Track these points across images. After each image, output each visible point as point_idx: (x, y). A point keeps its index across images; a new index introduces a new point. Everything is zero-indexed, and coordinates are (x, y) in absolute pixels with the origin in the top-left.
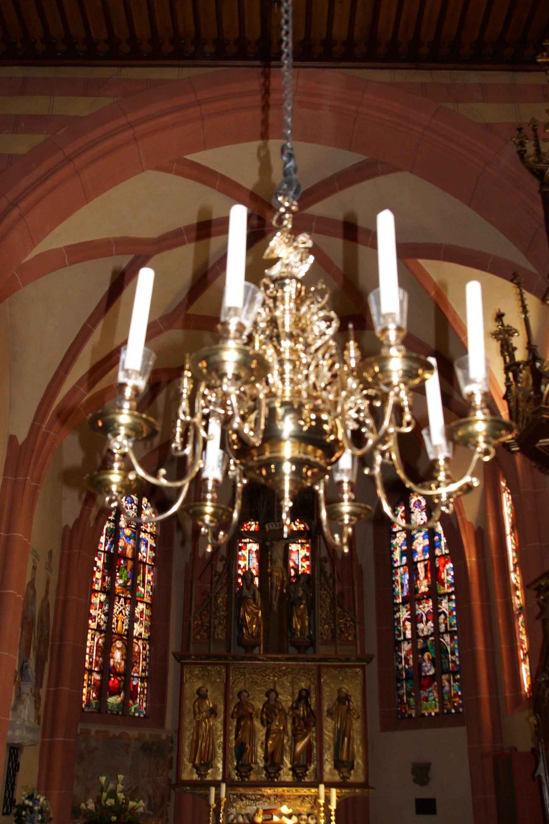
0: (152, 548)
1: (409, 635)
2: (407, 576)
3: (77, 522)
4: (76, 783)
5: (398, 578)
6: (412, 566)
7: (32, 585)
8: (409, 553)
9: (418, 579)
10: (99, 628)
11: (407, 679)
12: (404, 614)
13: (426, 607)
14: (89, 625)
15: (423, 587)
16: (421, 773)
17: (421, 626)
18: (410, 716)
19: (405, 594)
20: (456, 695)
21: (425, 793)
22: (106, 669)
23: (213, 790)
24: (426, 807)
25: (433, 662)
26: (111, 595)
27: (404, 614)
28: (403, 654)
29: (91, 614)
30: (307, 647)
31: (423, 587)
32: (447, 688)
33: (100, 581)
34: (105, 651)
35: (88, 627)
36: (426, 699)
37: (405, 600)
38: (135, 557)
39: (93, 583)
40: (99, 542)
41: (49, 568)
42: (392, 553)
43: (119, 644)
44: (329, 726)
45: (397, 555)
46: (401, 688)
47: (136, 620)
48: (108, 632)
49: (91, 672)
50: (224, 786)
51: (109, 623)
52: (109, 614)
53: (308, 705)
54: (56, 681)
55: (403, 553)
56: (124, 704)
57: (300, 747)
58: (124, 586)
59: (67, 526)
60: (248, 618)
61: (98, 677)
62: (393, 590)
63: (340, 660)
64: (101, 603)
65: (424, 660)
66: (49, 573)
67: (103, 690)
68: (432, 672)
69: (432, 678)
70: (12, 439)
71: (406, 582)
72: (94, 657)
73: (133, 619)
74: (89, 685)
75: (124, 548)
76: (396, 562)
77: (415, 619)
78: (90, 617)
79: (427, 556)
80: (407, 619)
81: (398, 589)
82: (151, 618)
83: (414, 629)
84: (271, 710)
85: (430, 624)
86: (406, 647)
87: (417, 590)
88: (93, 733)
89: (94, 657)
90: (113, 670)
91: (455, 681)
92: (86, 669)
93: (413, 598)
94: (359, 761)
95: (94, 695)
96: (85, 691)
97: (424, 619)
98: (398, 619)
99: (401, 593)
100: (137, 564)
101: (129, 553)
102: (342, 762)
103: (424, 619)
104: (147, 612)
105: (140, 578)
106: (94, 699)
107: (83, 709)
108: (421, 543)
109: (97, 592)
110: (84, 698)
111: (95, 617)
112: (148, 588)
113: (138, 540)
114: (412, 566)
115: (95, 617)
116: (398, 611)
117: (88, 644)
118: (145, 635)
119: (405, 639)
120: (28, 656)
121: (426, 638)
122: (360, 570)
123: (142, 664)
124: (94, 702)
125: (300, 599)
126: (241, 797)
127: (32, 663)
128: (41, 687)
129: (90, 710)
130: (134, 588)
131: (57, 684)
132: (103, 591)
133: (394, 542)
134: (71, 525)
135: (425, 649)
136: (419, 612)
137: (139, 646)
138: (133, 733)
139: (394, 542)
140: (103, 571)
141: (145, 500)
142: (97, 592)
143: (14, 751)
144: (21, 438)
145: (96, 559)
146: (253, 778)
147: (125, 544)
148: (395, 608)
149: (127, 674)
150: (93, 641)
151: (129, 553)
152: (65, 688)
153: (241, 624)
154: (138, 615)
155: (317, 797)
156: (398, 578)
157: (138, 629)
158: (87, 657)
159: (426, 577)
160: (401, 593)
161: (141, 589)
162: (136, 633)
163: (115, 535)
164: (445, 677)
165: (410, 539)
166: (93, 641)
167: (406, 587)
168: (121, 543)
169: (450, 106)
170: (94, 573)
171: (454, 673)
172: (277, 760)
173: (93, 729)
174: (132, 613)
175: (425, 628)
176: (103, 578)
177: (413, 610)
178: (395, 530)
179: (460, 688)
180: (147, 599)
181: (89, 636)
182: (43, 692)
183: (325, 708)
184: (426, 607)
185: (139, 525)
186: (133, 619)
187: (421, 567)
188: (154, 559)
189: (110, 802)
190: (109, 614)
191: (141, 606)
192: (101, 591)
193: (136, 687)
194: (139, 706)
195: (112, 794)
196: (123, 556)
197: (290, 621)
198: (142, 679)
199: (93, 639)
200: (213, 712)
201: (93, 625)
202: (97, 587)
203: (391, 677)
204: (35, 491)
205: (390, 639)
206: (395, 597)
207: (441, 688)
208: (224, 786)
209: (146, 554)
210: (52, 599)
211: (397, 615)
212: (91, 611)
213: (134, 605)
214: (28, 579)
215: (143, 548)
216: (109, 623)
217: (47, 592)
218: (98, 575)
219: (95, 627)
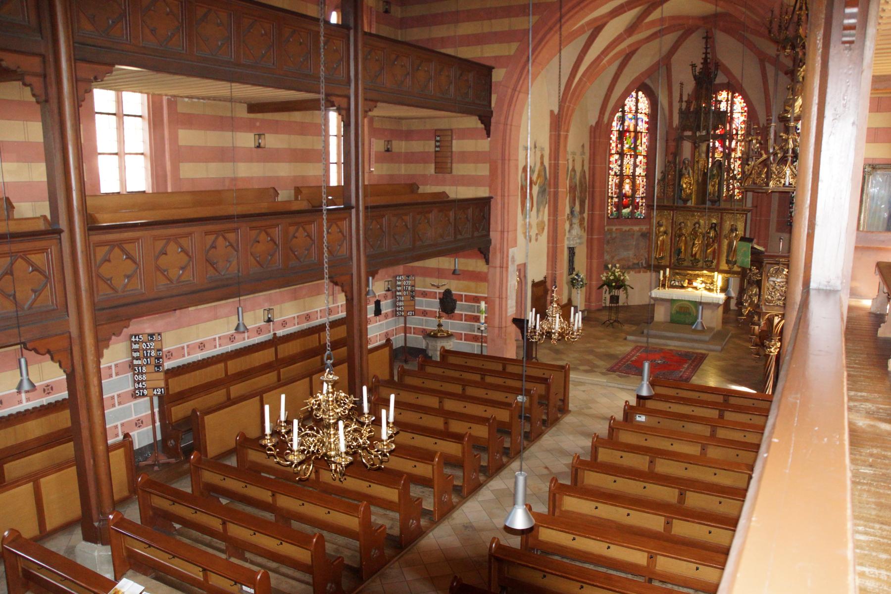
0: (646, 123)
3: (597, 123)
4: (605, 254)
7: (574, 170)
10: (616, 174)
22: (621, 195)
23: (662, 272)
26: (622, 154)
30: (715, 202)
34: (620, 186)
35: (609, 174)
38: (635, 131)
39: (610, 150)
40: (611, 126)
41: (583, 153)
43: (628, 181)
47: (637, 166)
48: (621, 176)
49: (612, 198)
50: (668, 270)
51: (621, 170)
52: (621, 166)
54: (592, 208)
56: (632, 212)
58: (630, 148)
60: (684, 186)
61: (616, 200)
64: (616, 161)
67: (619, 206)
70: (552, 112)
73: (635, 166)
75: (629, 126)
78: (610, 169)
82: (647, 164)
84: (694, 234)
90: (625, 195)
100: (636, 132)
101: (632, 129)
104: (645, 161)
105: (639, 142)
112: (644, 146)
113: (637, 119)
118: (643, 174)
120: (574, 204)
123: (642, 190)
124: (615, 213)
126: (677, 274)
127: (577, 208)
130: (636, 147)
131: (592, 210)
132: (617, 153)
134: (594, 124)
137: (639, 181)
138: (636, 228)
141: (640, 93)
143: (572, 251)
144: (556, 111)
146: (685, 264)
147: (629, 123)
149: (633, 196)
150: (613, 181)
151: (632, 129)
152: (597, 213)
153: (681, 189)
154: (638, 163)
157: (639, 171)
161: (639, 147)
162: (637, 174)
163: (622, 120)
166: (613, 181)
168: (626, 124)
173: (614, 228)
174: (635, 163)
176: (617, 146)
180: (644, 153)
182: (585, 215)
185: (636, 112)
186: (635, 166)
188: (647, 129)
189: (612, 278)
190: (621, 166)
191: (640, 158)
193: (638, 203)
194: (641, 212)
195: (613, 273)
196: (628, 131)
198: (642, 198)
200: (665, 233)
201: (612, 173)
202: (613, 152)
204: (566, 137)
208: (668, 270)
209: (642, 127)
210: (586, 168)
213: (636, 156)
214: (570, 168)
215: (640, 123)
216: (621, 170)
217: (583, 166)
218: (614, 145)
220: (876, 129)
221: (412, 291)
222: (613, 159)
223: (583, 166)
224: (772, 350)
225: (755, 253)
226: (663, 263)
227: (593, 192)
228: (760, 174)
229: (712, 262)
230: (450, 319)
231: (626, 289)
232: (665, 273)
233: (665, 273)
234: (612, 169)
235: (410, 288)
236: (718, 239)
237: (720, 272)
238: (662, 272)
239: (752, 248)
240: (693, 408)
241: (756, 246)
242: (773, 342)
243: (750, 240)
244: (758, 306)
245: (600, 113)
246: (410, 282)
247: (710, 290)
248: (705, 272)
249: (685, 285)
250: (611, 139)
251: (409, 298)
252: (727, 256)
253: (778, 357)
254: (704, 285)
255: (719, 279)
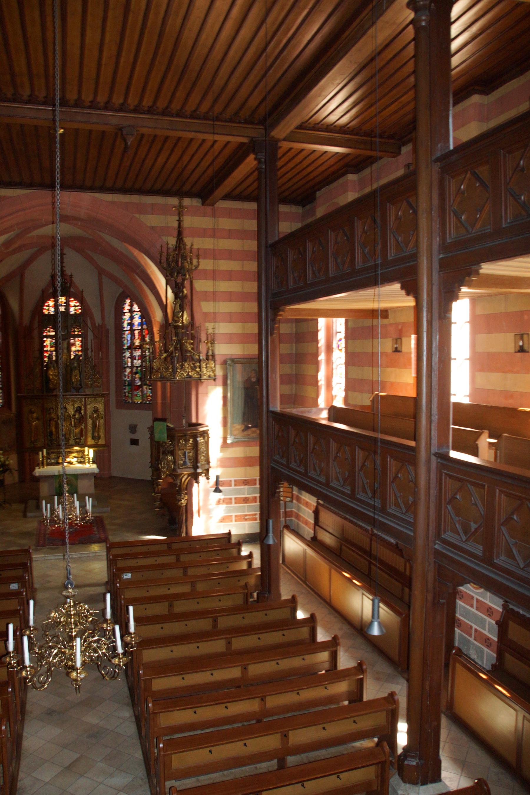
1: (129, 365)
2: (129, 336)
5: (125, 336)
6: (132, 331)
8: (131, 324)
9: (135, 339)
11: (128, 385)
12: (127, 354)
13: (138, 353)
15: (137, 343)
16: (133, 429)
17: (135, 361)
18: (129, 402)
19: (129, 345)
20: (149, 396)
21: (135, 437)
24: (135, 442)
25: (141, 379)
27: (127, 354)
28: (127, 373)
31: (137, 343)
32: (145, 392)
36: (136, 395)
37: (129, 348)
42: (124, 322)
44: (90, 422)
45: (125, 325)
46: (125, 389)
50: (45, 451)
53: (80, 413)
55: (129, 324)
57: (77, 430)
60: (51, 377)
62: (123, 342)
63: (93, 395)
65: (136, 378)
68: (139, 384)
69: (140, 387)
71: (129, 339)
76: (124, 328)
77: (133, 358)
79: (140, 328)
80: (129, 357)
81: (125, 342)
83: (132, 362)
85: (140, 361)
86: (128, 370)
87: (134, 344)
91: (150, 389)
93: (132, 347)
94: (102, 435)
97: (137, 358)
98: (125, 356)
99: (127, 344)
102: (95, 437)
103: (137, 358)
108: (137, 320)
114: (132, 331)
116: (125, 353)
119: (128, 367)
121: (137, 367)
122: (107, 331)
125: (75, 367)
133: (124, 317)
135: (136, 373)
136: (134, 355)
139: (124, 317)
148: (123, 351)
155: (84, 452)
156: (125, 336)
159: (138, 338)
160: (127, 344)
164: (145, 387)
165: (132, 318)
167: (129, 341)
169: (137, 216)
171: (150, 386)
172: (68, 436)
175: (137, 363)
177: (131, 353)
178: (125, 311)
179: (151, 393)
183: (88, 415)
184: (138, 353)
187: (136, 332)
197: (71, 377)
203: (120, 383)
205: (121, 367)
206: (124, 345)
207: (142, 392)
208: (45, 451)
211: (124, 355)
220: (231, 334)
224: (183, 501)
225: (169, 429)
226: (39, 444)
228: (167, 369)
229: (81, 439)
231: (11, 472)
232: (43, 454)
233: (43, 454)
236: (82, 419)
237: (90, 447)
238: (40, 453)
239: (167, 426)
240: (156, 559)
241: (169, 425)
242: (183, 496)
243: (164, 420)
244: (174, 470)
247: (80, 463)
248: (76, 448)
249: (60, 461)
252: (93, 433)
253: (186, 506)
254: (76, 459)
255: (90, 453)
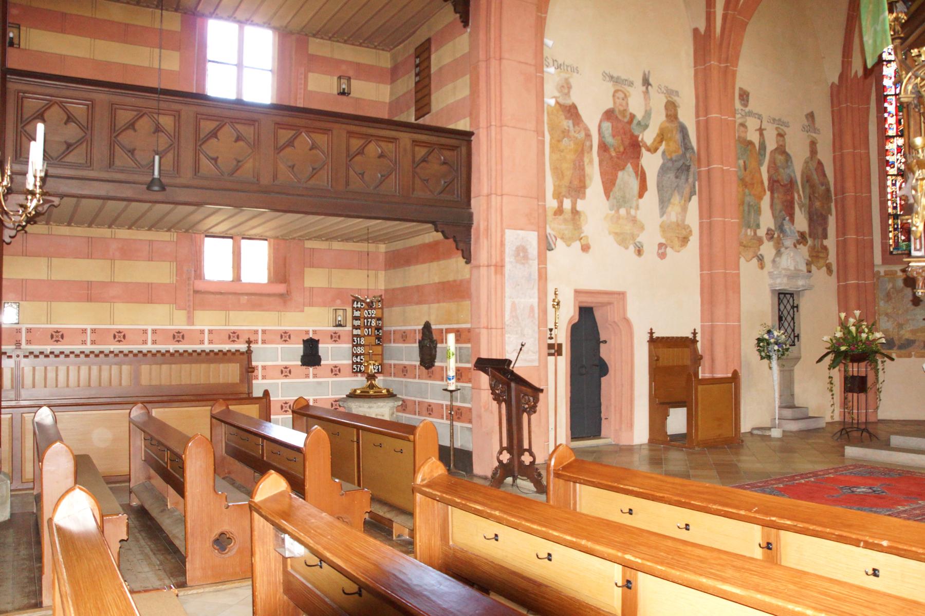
3: (841, 77)
7: (781, 150)
14: (887, 172)
29: (888, 161)
33: (895, 126)
59: (833, 84)
64: (899, 149)
66: (814, 135)
72: (898, 202)
74: (895, 229)
88: (882, 274)
89: (898, 202)
92: (890, 214)
95: (903, 238)
96: (891, 235)
106: (904, 241)
107: (891, 253)
109: (893, 137)
110: (891, 242)
111: (893, 163)
115: (893, 163)
117: (889, 190)
128: (825, 236)
129: (900, 252)
134: (836, 82)
140: (897, 115)
142: (893, 137)
144: (702, 30)
145: (886, 105)
158: (889, 203)
170: (886, 119)
176: (898, 122)
181: (889, 183)
182: (831, 242)
192: (897, 136)
199: (894, 185)
201: (893, 171)
202: (891, 133)
212: (888, 158)
214: (771, 146)
219: (896, 173)
221: (378, 329)
222: (891, 146)
223: (813, 152)
227: (843, 199)
230: (430, 377)
234: (892, 165)
235: (374, 323)
245: (844, 56)
246: (373, 313)
250: (885, 109)
251: (373, 340)
